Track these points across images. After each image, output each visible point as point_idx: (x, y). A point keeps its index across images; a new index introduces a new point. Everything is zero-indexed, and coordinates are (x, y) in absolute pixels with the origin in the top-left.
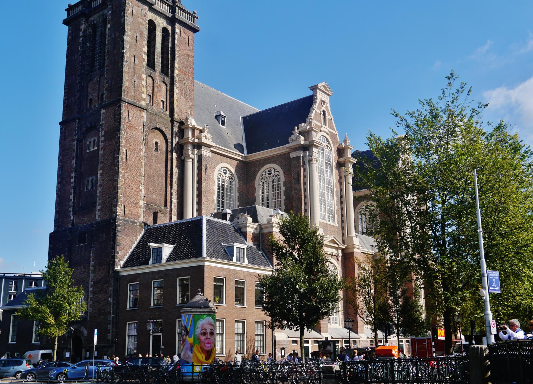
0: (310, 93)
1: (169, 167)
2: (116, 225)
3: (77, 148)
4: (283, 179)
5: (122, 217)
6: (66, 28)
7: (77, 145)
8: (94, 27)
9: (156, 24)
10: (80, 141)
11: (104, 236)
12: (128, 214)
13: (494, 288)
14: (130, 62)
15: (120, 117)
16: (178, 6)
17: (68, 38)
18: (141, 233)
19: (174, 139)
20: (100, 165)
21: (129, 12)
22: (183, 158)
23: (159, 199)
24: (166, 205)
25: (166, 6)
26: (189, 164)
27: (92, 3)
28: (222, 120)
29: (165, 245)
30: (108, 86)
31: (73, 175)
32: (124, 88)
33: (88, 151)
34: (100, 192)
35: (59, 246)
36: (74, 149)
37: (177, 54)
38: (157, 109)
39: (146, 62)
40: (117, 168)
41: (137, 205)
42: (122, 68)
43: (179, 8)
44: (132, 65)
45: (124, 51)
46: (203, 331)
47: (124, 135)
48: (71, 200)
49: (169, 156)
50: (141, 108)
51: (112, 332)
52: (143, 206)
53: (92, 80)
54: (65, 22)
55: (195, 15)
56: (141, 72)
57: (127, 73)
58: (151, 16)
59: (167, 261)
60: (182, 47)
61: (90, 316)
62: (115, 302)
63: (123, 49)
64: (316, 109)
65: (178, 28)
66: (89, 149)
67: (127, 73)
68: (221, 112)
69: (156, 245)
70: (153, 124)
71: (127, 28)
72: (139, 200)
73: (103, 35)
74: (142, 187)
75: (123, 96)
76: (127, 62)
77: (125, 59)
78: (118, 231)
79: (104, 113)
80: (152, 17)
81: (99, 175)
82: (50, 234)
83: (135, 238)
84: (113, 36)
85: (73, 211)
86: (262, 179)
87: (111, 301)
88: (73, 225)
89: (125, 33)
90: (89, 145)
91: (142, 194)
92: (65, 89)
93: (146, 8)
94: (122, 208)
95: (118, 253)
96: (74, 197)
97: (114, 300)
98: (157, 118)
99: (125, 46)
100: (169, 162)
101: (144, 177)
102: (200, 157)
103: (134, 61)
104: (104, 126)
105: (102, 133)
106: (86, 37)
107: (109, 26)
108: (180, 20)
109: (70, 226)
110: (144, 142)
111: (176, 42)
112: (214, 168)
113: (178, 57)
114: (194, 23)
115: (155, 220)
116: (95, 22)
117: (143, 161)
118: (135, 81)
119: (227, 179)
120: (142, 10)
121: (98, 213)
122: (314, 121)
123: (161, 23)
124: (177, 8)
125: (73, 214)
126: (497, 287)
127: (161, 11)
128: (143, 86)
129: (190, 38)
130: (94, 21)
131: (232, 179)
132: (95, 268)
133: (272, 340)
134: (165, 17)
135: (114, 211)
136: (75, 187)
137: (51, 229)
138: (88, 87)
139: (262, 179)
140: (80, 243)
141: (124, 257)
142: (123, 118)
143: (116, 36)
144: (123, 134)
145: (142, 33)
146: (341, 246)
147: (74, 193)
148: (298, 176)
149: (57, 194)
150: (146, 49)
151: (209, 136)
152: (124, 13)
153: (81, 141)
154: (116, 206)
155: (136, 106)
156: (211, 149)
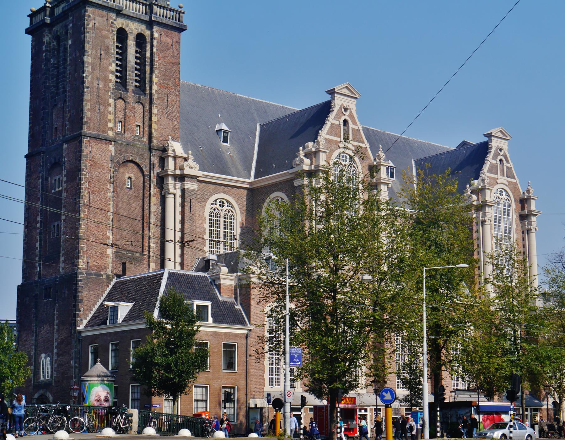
0: (328, 98)
1: (146, 205)
2: (77, 280)
3: (42, 187)
5: (85, 269)
6: (29, 37)
7: (42, 184)
9: (128, 32)
11: (67, 292)
12: (93, 265)
13: (295, 363)
14: (92, 88)
15: (81, 154)
16: (155, 5)
17: (32, 52)
18: (108, 286)
19: (152, 172)
22: (163, 193)
25: (141, 6)
26: (170, 201)
27: (55, 10)
28: (224, 136)
29: (121, 303)
30: (70, 115)
31: (39, 219)
32: (85, 120)
33: (53, 191)
35: (26, 301)
36: (39, 188)
37: (156, 64)
38: (130, 137)
41: (104, 255)
42: (83, 95)
43: (158, 6)
44: (95, 90)
45: (84, 75)
46: (97, 398)
47: (86, 175)
48: (37, 248)
49: (147, 193)
50: (107, 140)
52: (111, 255)
53: (56, 105)
54: (28, 31)
55: (181, 10)
56: (107, 97)
58: (120, 22)
59: (123, 321)
61: (55, 380)
62: (77, 365)
63: (83, 73)
65: (157, 32)
66: (55, 189)
67: (89, 101)
70: (124, 157)
71: (87, 46)
76: (88, 87)
77: (86, 85)
78: (79, 286)
79: (66, 148)
80: (123, 24)
81: (62, 221)
82: (18, 286)
83: (100, 293)
84: (74, 55)
87: (73, 365)
88: (39, 278)
89: (86, 54)
90: (55, 183)
92: (30, 115)
93: (113, 15)
95: (80, 311)
96: (40, 244)
98: (129, 149)
99: (85, 69)
100: (146, 200)
101: (112, 221)
102: (183, 190)
104: (66, 163)
105: (65, 172)
106: (50, 52)
107: (70, 42)
109: (37, 279)
110: (112, 180)
111: (155, 50)
112: (206, 201)
113: (157, 68)
114: (179, 21)
116: (59, 34)
117: (111, 203)
118: (99, 109)
119: (224, 212)
120: (107, 20)
121: (62, 265)
124: (155, 7)
126: (298, 362)
127: (133, 15)
128: (110, 113)
129: (175, 40)
131: (232, 212)
132: (59, 328)
133: (246, 407)
134: (141, 21)
137: (19, 281)
138: (53, 113)
141: (88, 315)
142: (84, 155)
144: (85, 174)
145: (107, 49)
147: (41, 241)
149: (24, 240)
150: (113, 67)
151: (194, 164)
152: (84, 29)
153: (47, 179)
154: (78, 258)
155: (101, 139)
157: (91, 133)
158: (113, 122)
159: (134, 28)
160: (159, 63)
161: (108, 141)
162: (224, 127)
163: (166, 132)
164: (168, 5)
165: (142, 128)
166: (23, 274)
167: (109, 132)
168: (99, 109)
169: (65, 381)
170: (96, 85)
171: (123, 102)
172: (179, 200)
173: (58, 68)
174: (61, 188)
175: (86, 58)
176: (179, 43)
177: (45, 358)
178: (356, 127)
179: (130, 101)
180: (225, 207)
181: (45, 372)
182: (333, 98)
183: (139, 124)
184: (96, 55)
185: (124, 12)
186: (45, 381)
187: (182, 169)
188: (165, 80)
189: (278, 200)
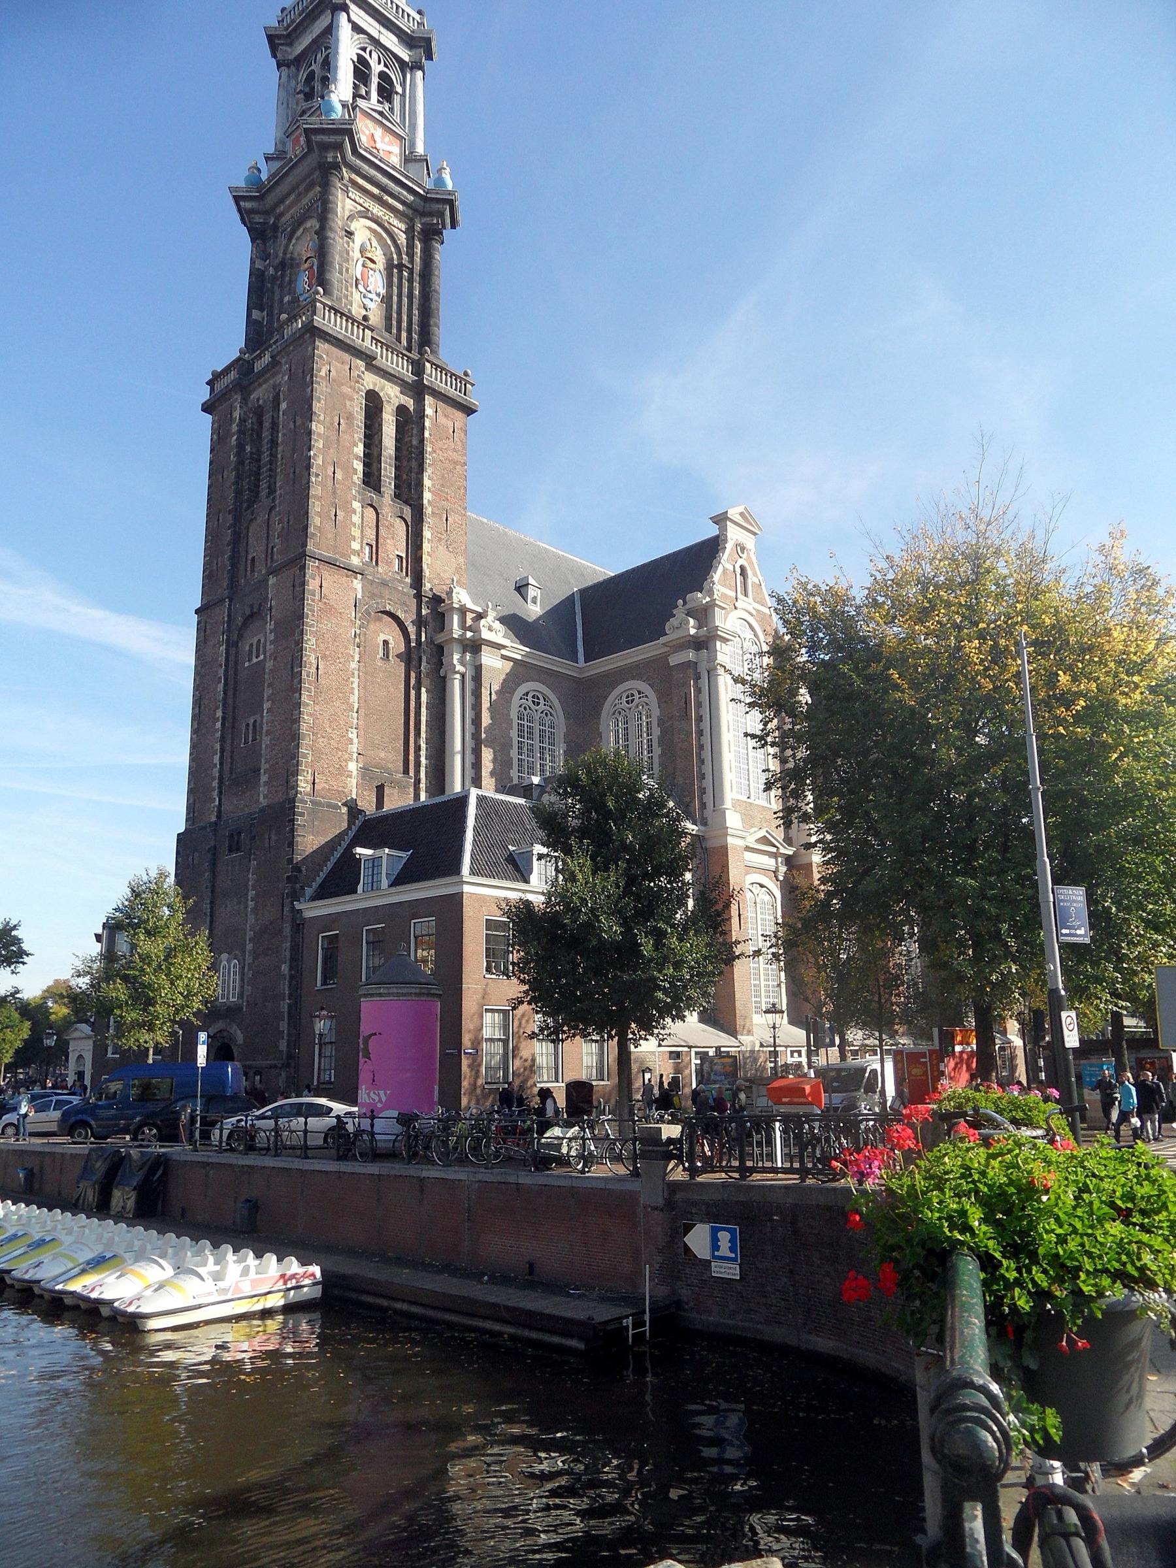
0: (713, 531)
3: (227, 659)
4: (656, 712)
8: (259, 412)
10: (232, 645)
12: (323, 789)
16: (428, 361)
20: (268, 692)
21: (323, 373)
22: (442, 673)
23: (391, 757)
24: (406, 771)
30: (283, 527)
31: (219, 714)
32: (311, 530)
33: (247, 664)
34: (267, 746)
39: (361, 475)
40: (297, 695)
41: (342, 771)
43: (433, 364)
44: (330, 483)
45: (312, 453)
47: (312, 626)
51: (289, 1035)
52: (355, 773)
53: (255, 518)
54: (207, 408)
55: (467, 379)
57: (320, 498)
58: (371, 381)
59: (391, 886)
60: (440, 444)
63: (310, 450)
64: (726, 562)
67: (320, 498)
68: (530, 578)
69: (369, 852)
70: (378, 603)
71: (317, 406)
72: (346, 761)
73: (274, 425)
74: (353, 735)
75: (310, 547)
76: (317, 475)
77: (313, 470)
78: (299, 825)
80: (375, 384)
84: (292, 425)
85: (220, 787)
86: (614, 714)
87: (286, 972)
88: (219, 816)
90: (250, 651)
91: (354, 748)
93: (361, 364)
94: (310, 778)
96: (222, 757)
97: (291, 968)
98: (386, 592)
103: (334, 473)
105: (270, 626)
107: (284, 406)
108: (434, 390)
109: (214, 819)
111: (427, 434)
115: (380, 803)
116: (261, 402)
117: (356, 680)
118: (336, 515)
120: (350, 369)
121: (263, 790)
122: (719, 587)
123: (392, 395)
124: (428, 365)
125: (220, 793)
126: (1079, 928)
128: (354, 525)
130: (258, 400)
135: (292, 784)
136: (223, 739)
139: (614, 714)
140: (230, 851)
141: (314, 880)
142: (308, 590)
143: (297, 424)
145: (350, 417)
146: (782, 851)
147: (222, 751)
148: (238, 539)
150: (360, 449)
152: (312, 377)
156: (503, 652)
158: (359, 540)
163: (445, 571)
165: (404, 561)
166: (188, 814)
167: (352, 557)
169: (269, 1005)
172: (469, 685)
173: (259, 460)
174: (262, 657)
175: (314, 426)
177: (229, 961)
179: (387, 514)
180: (541, 707)
181: (229, 987)
182: (724, 529)
183: (401, 554)
186: (228, 1004)
187: (476, 630)
188: (443, 486)
189: (633, 695)
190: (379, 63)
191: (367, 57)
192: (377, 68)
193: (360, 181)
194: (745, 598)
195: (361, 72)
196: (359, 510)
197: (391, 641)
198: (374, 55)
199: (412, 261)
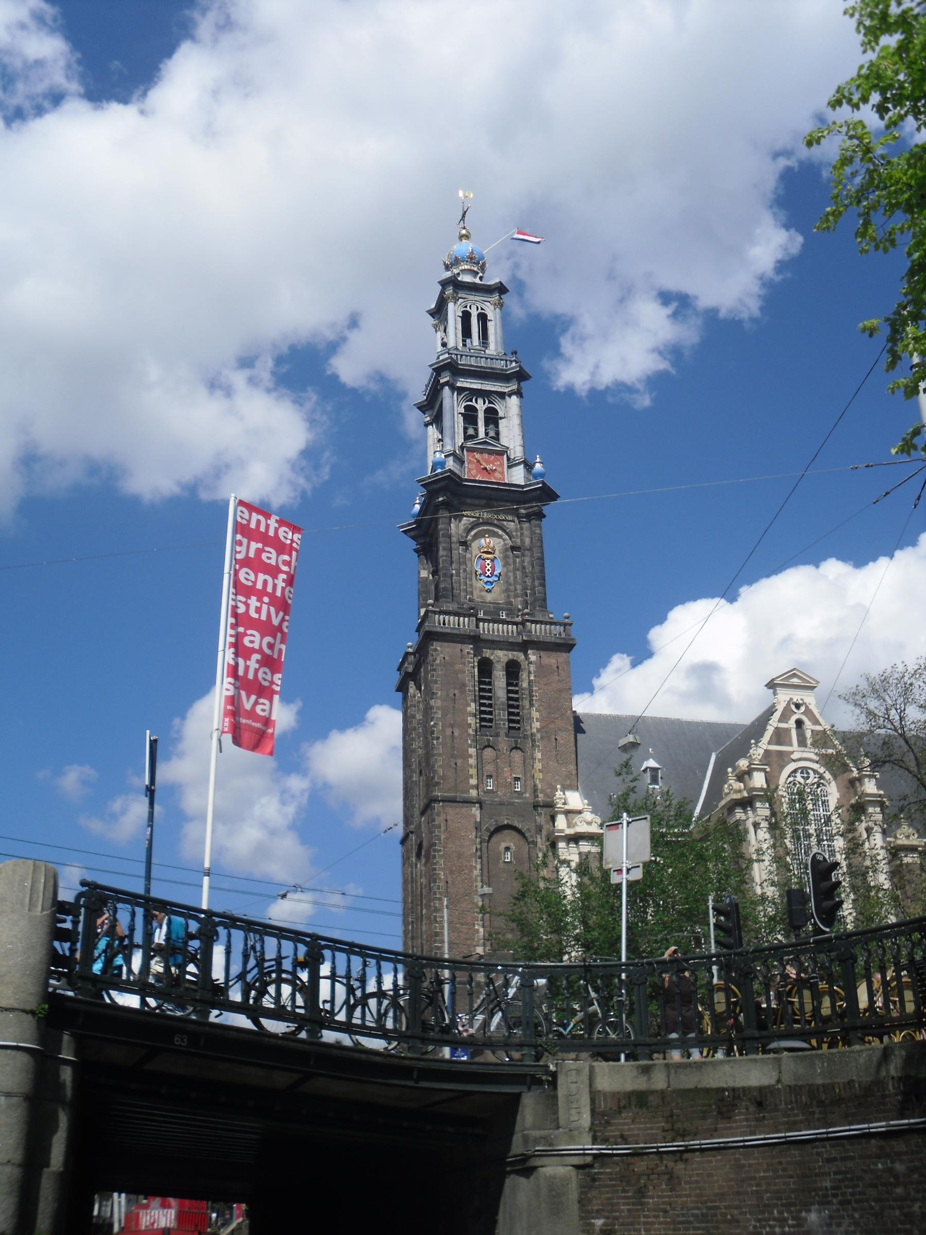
6: (401, 693)
43: (532, 622)
57: (439, 755)
65: (534, 654)
67: (439, 755)
76: (438, 738)
110: (479, 853)
111: (532, 678)
124: (528, 624)
128: (471, 766)
145: (464, 685)
150: (472, 707)
157: (445, 796)
159: (500, 657)
160: (540, 693)
161: (469, 802)
162: (652, 763)
164: (552, 618)
167: (471, 791)
168: (456, 764)
170: (448, 731)
171: (492, 750)
176: (568, 663)
178: (818, 728)
179: (503, 748)
184: (447, 696)
185: (484, 637)
190: (484, 403)
191: (473, 403)
192: (481, 406)
193: (469, 501)
194: (802, 749)
195: (470, 416)
196: (474, 754)
197: (513, 847)
198: (480, 401)
199: (522, 541)
